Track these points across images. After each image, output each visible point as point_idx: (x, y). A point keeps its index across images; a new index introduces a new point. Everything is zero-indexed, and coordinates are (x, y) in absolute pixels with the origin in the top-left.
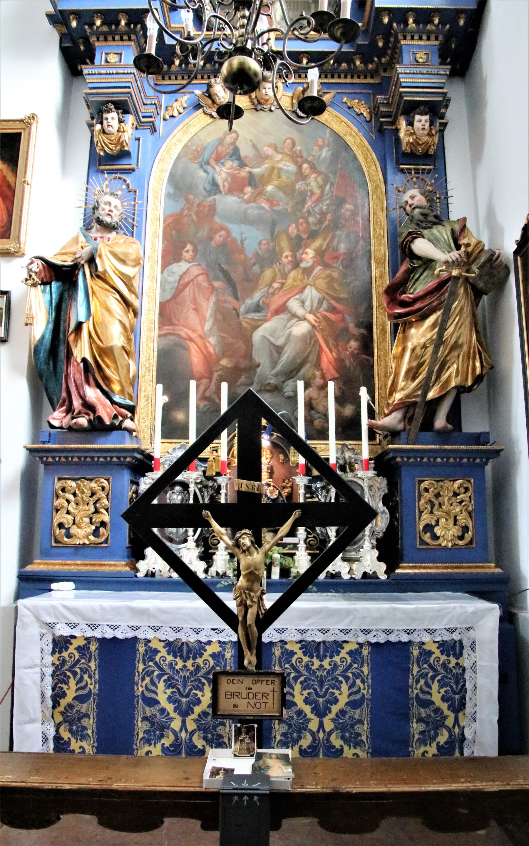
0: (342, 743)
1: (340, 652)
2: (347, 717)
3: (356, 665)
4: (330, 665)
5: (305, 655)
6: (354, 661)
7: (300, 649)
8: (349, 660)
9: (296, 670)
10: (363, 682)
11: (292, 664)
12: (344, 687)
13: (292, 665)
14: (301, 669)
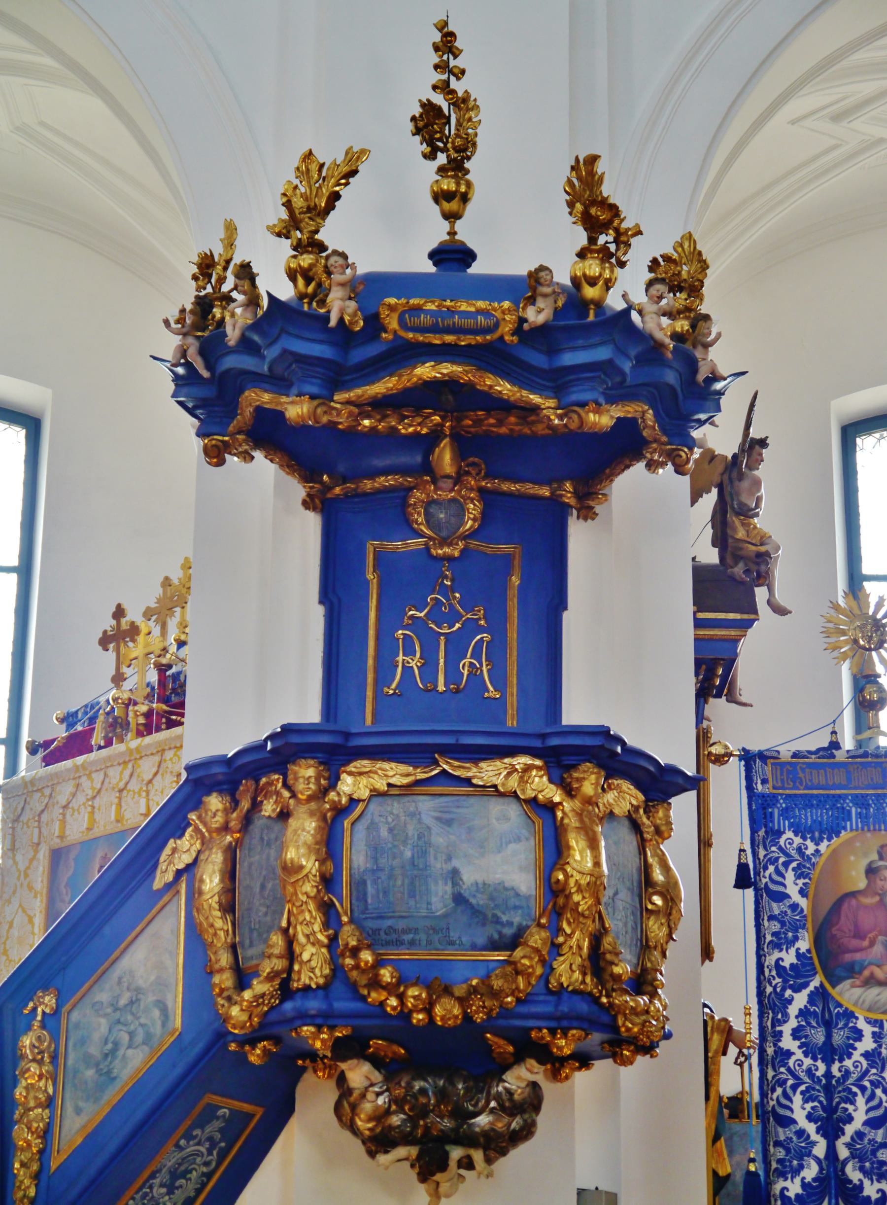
0: (861, 1176)
1: (852, 1054)
2: (866, 1141)
3: (874, 1071)
4: (840, 1071)
5: (806, 1056)
7: (800, 1047)
8: (865, 1064)
11: (789, 1067)
12: (860, 1100)
13: (789, 1070)
14: (802, 1075)
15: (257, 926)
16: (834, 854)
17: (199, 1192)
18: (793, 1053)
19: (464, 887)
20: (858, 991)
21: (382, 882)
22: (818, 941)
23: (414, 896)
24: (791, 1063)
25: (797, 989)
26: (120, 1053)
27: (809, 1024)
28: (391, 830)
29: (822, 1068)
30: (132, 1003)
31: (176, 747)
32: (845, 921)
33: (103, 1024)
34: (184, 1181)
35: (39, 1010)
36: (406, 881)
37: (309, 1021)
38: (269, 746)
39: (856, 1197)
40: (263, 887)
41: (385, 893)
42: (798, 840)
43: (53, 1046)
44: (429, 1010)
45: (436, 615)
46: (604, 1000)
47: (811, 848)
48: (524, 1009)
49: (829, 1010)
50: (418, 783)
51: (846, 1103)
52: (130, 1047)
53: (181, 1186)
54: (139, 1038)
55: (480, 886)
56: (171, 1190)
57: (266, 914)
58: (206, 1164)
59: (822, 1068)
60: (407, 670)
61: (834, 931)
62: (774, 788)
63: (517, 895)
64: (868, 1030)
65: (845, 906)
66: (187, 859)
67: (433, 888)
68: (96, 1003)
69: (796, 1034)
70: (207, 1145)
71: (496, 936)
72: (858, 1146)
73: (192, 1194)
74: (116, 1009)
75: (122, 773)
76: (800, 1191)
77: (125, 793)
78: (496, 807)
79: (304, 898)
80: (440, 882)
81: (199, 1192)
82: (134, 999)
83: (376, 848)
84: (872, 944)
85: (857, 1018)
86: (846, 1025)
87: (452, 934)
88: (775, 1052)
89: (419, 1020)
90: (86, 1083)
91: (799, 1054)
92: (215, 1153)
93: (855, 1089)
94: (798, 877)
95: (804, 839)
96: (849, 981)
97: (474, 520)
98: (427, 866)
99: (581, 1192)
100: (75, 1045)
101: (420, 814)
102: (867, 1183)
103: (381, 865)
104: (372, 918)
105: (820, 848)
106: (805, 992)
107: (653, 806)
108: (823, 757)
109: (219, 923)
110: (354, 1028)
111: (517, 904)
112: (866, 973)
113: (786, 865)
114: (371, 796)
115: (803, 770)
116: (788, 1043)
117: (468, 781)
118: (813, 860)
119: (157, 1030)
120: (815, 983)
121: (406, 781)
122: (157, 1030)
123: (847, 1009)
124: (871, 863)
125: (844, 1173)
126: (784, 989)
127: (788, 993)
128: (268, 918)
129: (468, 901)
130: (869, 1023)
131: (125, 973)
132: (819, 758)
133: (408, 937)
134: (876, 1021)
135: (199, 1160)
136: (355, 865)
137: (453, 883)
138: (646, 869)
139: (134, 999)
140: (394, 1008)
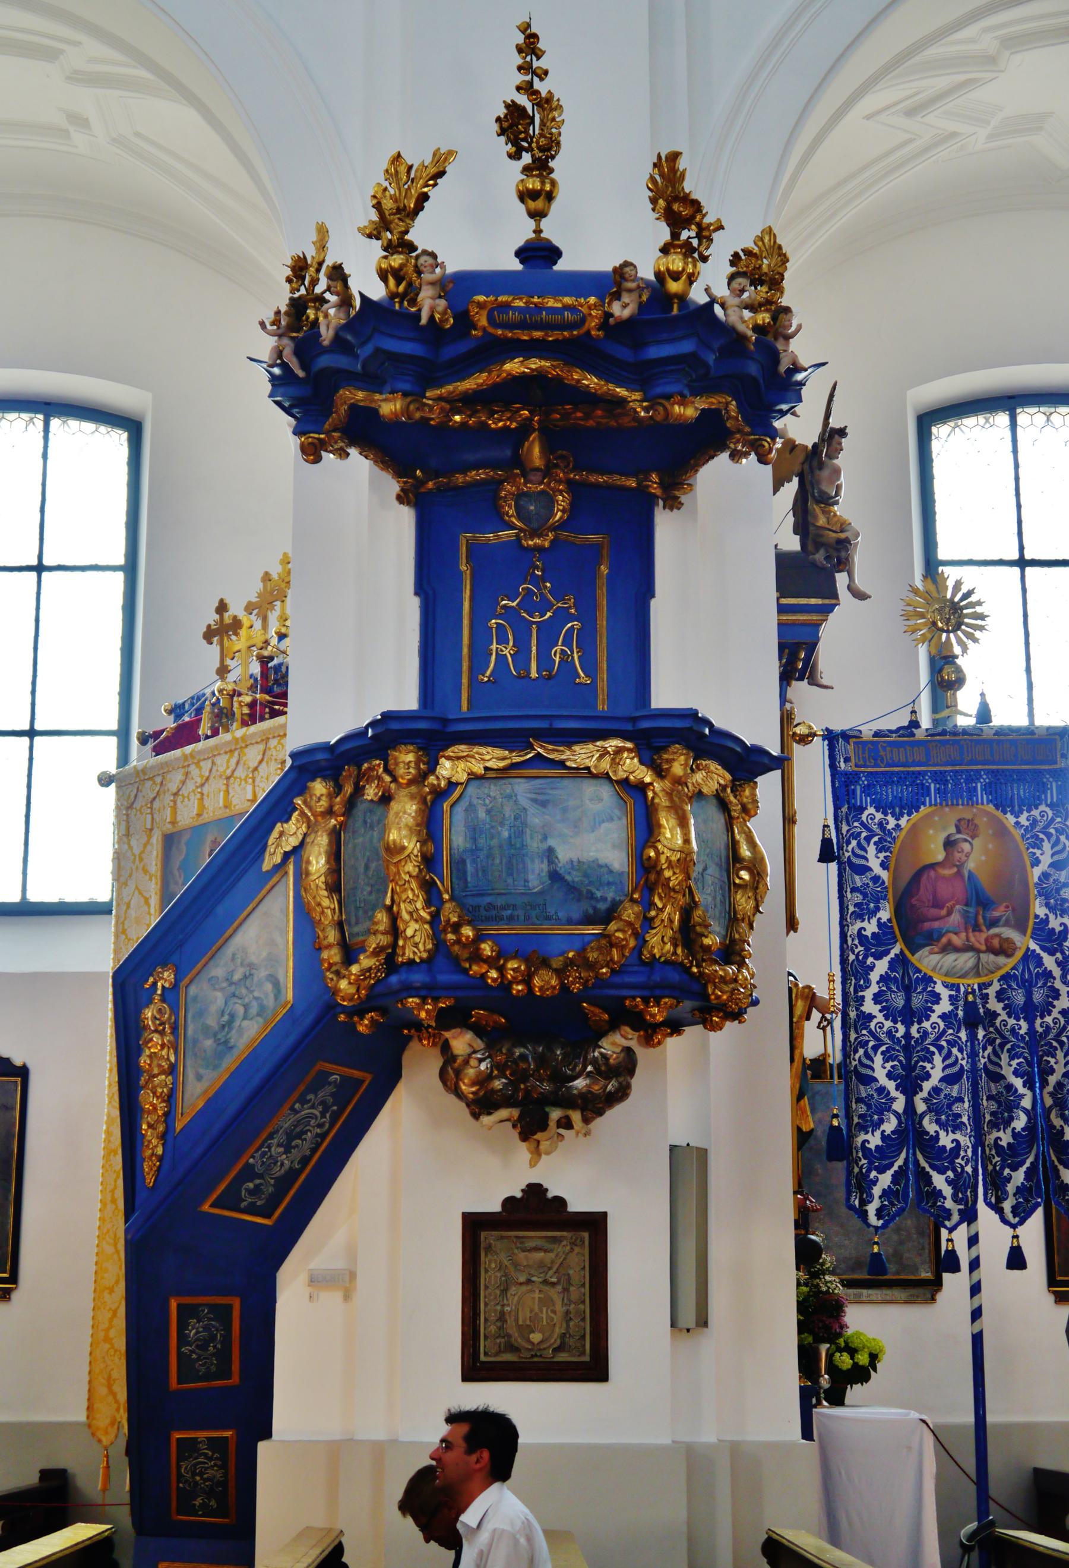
0: (937, 1128)
1: (930, 1016)
2: (942, 1095)
3: (951, 1031)
4: (919, 1032)
6: (948, 1026)
7: (880, 1011)
8: (942, 1025)
9: (876, 1038)
10: (961, 1050)
11: (871, 1030)
12: (938, 1059)
13: (870, 1032)
15: (362, 905)
16: (914, 829)
17: (314, 1151)
18: (875, 1017)
19: (560, 865)
20: (936, 958)
21: (481, 861)
22: (898, 911)
23: (512, 875)
24: (872, 1025)
25: (879, 956)
26: (237, 1024)
27: (889, 989)
28: (489, 812)
29: (901, 1030)
30: (245, 977)
31: (279, 736)
32: (924, 893)
33: (219, 999)
34: (300, 1142)
35: (159, 984)
36: (504, 860)
37: (413, 993)
38: (370, 733)
39: (933, 1147)
40: (367, 867)
41: (485, 872)
42: (879, 816)
43: (173, 1018)
44: (528, 981)
45: (528, 604)
46: (695, 970)
47: (892, 823)
48: (617, 979)
49: (909, 975)
50: (514, 766)
51: (924, 1062)
52: (245, 1018)
53: (297, 1146)
54: (254, 1009)
56: (288, 1149)
57: (370, 893)
58: (320, 1126)
59: (901, 1030)
60: (501, 658)
61: (914, 901)
62: (857, 766)
63: (611, 872)
64: (945, 993)
65: (924, 878)
66: (294, 842)
67: (530, 866)
68: (212, 977)
69: (877, 998)
70: (320, 1108)
71: (591, 911)
72: (935, 1101)
73: (308, 1153)
74: (231, 984)
75: (228, 761)
76: (880, 1143)
77: (232, 780)
78: (590, 788)
79: (407, 878)
80: (537, 861)
81: (314, 1151)
82: (247, 974)
83: (474, 829)
84: (949, 913)
85: (935, 983)
86: (924, 989)
87: (549, 910)
88: (857, 1015)
89: (518, 991)
90: (205, 1051)
91: (880, 1017)
92: (328, 1116)
93: (932, 1049)
94: (879, 851)
95: (886, 814)
96: (928, 948)
97: (563, 511)
98: (523, 846)
99: (673, 1148)
100: (194, 1017)
101: (516, 795)
102: (942, 1134)
103: (480, 845)
104: (473, 895)
105: (900, 822)
106: (886, 960)
107: (740, 786)
108: (903, 736)
109: (326, 902)
110: (457, 999)
111: (611, 880)
112: (944, 940)
113: (868, 839)
114: (469, 780)
115: (884, 748)
116: (870, 1007)
117: (562, 764)
118: (894, 834)
119: (270, 1002)
120: (895, 951)
121: (502, 764)
122: (270, 1002)
123: (925, 974)
124: (949, 836)
125: (920, 1123)
126: (866, 957)
127: (870, 960)
128: (373, 897)
129: (564, 878)
130: (946, 987)
131: (238, 950)
132: (899, 736)
133: (507, 913)
134: (953, 985)
135: (313, 1122)
136: (455, 845)
137: (549, 862)
138: (734, 845)
139: (247, 974)
140: (494, 980)
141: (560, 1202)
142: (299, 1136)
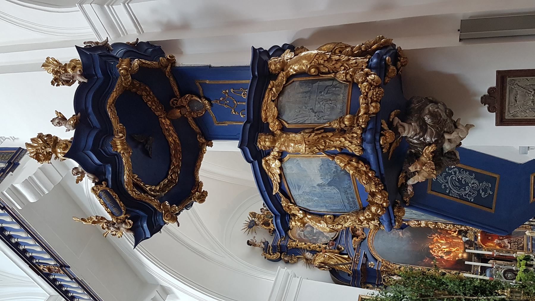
17: (466, 171)
23: (333, 197)
48: (374, 167)
55: (322, 177)
58: (455, 172)
81: (466, 171)
114: (297, 206)
133: (351, 199)
135: (454, 178)
141: (491, 90)
142: (460, 181)
